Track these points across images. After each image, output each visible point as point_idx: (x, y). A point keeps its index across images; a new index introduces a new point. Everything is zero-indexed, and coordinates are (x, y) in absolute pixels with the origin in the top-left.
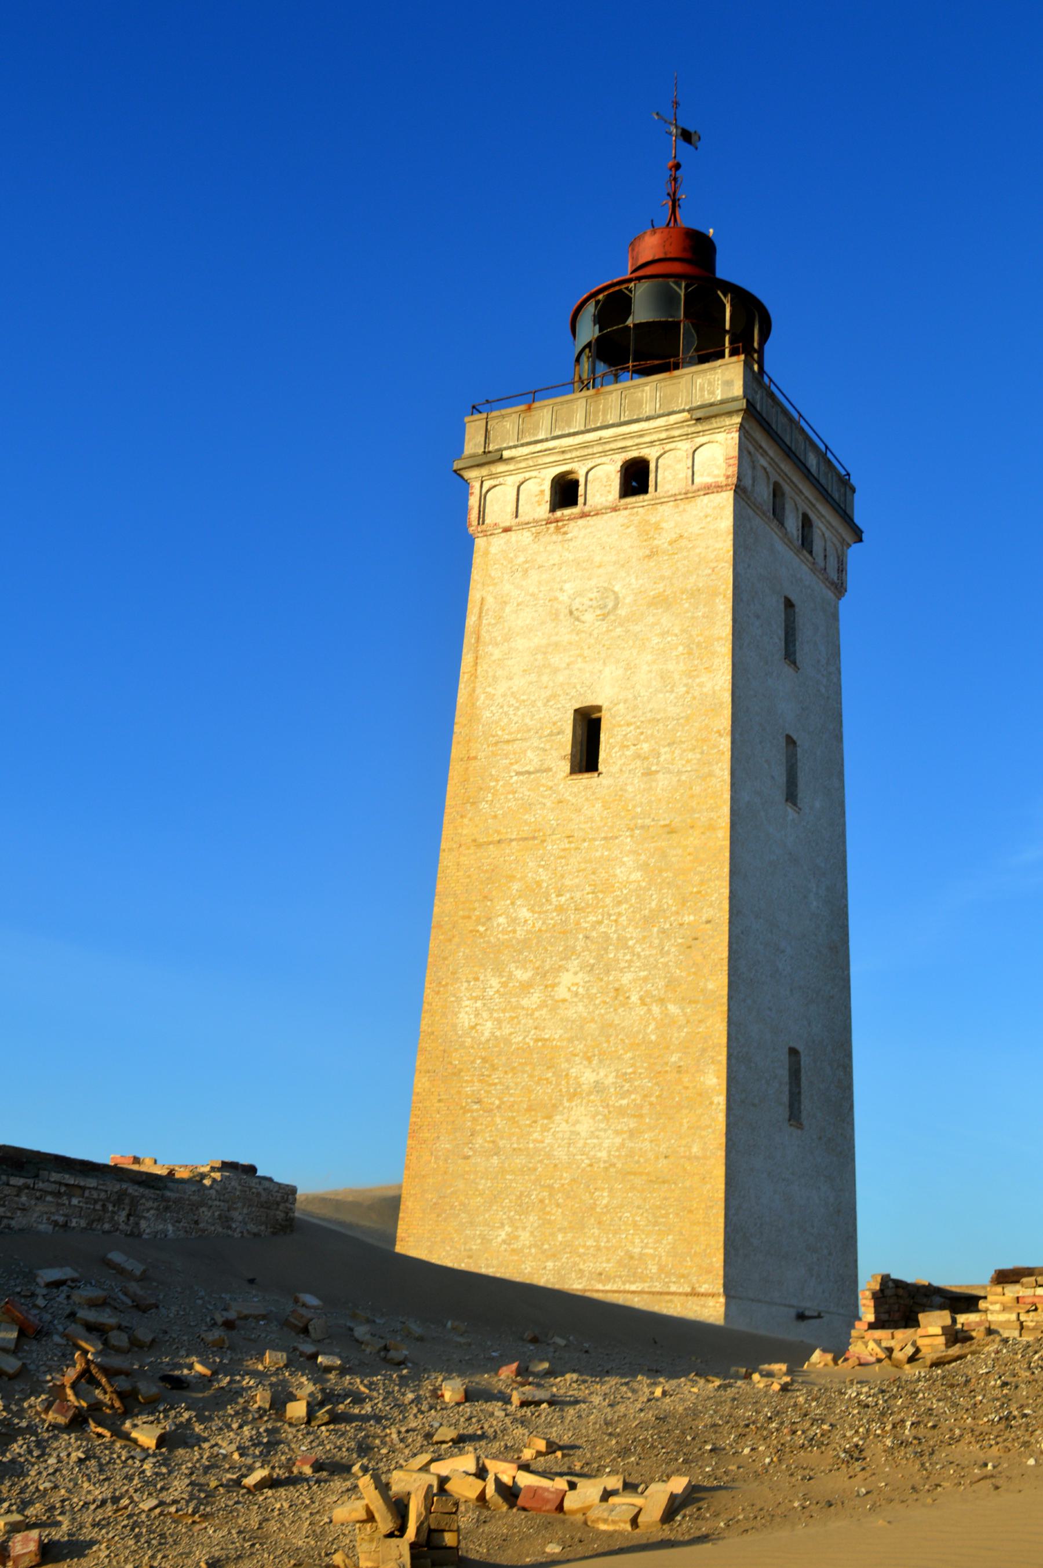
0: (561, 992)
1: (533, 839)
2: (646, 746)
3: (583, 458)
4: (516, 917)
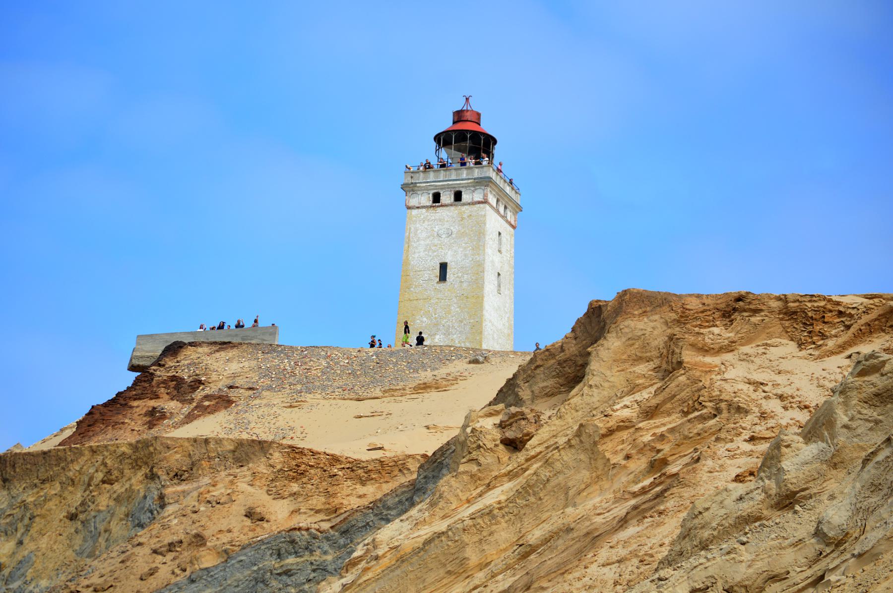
1: (427, 299)
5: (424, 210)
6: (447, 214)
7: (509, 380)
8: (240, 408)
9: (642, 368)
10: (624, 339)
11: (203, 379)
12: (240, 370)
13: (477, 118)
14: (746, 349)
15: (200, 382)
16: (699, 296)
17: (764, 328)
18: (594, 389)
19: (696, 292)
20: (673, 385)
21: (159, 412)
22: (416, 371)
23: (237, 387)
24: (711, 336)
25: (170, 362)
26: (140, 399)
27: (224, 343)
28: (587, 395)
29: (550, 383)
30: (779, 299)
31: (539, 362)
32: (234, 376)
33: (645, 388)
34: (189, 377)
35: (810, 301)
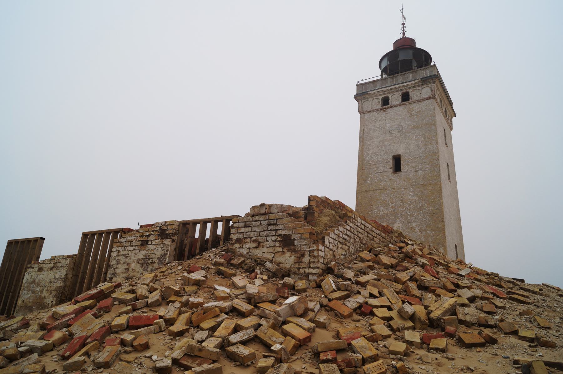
2: (414, 164)
3: (390, 93)
5: (375, 113)
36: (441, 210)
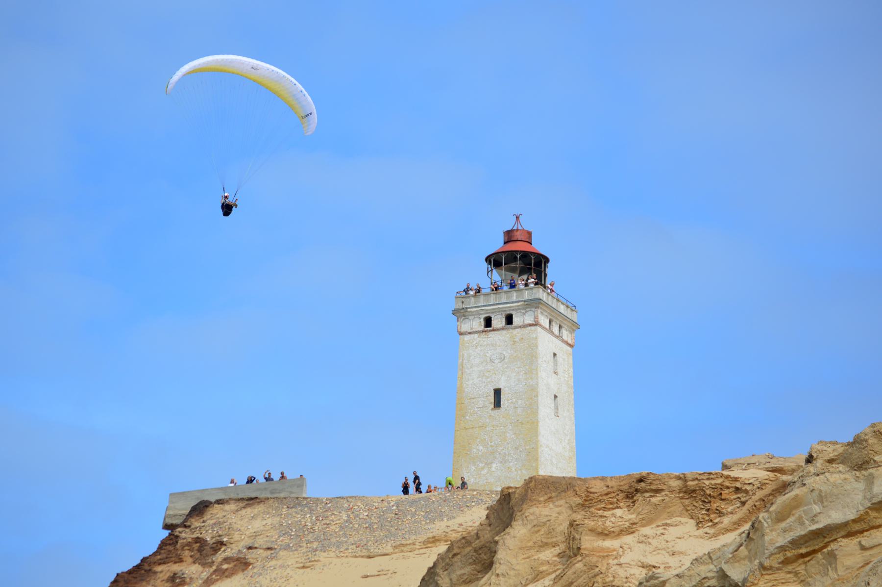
0: (493, 469)
4: (479, 449)
5: (476, 336)
6: (500, 338)
7: (430, 569)
8: (255, 571)
9: (548, 555)
10: (529, 527)
11: (225, 540)
12: (262, 528)
13: (528, 238)
14: (647, 530)
15: (222, 543)
16: (603, 479)
17: (665, 508)
18: (501, 578)
19: (600, 475)
20: (570, 572)
21: (180, 577)
22: (432, 521)
23: (256, 548)
24: (613, 519)
25: (196, 523)
26: (164, 563)
27: (251, 499)
28: (495, 584)
29: (468, 570)
30: (679, 478)
31: (456, 551)
32: (256, 535)
33: (549, 574)
34: (212, 538)
35: (708, 479)
36: (536, 449)
